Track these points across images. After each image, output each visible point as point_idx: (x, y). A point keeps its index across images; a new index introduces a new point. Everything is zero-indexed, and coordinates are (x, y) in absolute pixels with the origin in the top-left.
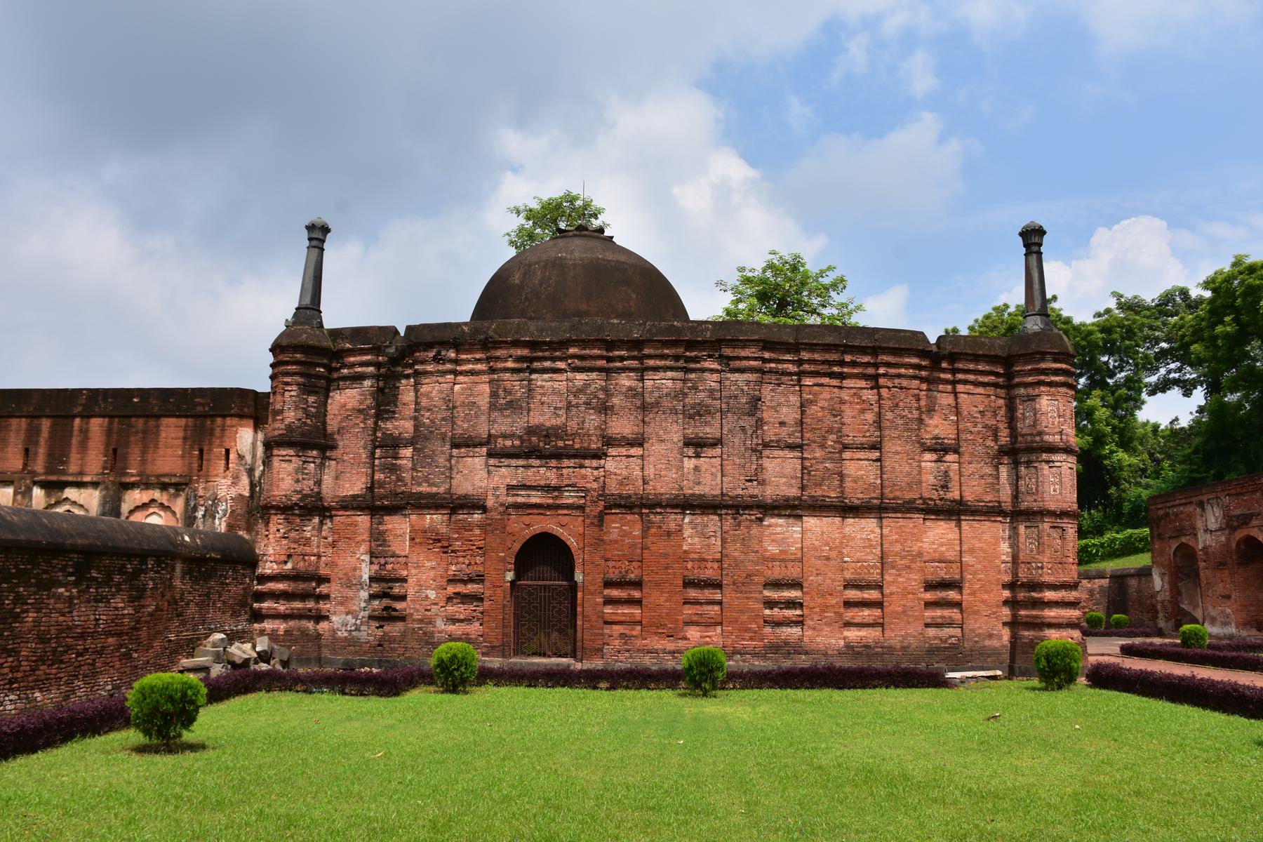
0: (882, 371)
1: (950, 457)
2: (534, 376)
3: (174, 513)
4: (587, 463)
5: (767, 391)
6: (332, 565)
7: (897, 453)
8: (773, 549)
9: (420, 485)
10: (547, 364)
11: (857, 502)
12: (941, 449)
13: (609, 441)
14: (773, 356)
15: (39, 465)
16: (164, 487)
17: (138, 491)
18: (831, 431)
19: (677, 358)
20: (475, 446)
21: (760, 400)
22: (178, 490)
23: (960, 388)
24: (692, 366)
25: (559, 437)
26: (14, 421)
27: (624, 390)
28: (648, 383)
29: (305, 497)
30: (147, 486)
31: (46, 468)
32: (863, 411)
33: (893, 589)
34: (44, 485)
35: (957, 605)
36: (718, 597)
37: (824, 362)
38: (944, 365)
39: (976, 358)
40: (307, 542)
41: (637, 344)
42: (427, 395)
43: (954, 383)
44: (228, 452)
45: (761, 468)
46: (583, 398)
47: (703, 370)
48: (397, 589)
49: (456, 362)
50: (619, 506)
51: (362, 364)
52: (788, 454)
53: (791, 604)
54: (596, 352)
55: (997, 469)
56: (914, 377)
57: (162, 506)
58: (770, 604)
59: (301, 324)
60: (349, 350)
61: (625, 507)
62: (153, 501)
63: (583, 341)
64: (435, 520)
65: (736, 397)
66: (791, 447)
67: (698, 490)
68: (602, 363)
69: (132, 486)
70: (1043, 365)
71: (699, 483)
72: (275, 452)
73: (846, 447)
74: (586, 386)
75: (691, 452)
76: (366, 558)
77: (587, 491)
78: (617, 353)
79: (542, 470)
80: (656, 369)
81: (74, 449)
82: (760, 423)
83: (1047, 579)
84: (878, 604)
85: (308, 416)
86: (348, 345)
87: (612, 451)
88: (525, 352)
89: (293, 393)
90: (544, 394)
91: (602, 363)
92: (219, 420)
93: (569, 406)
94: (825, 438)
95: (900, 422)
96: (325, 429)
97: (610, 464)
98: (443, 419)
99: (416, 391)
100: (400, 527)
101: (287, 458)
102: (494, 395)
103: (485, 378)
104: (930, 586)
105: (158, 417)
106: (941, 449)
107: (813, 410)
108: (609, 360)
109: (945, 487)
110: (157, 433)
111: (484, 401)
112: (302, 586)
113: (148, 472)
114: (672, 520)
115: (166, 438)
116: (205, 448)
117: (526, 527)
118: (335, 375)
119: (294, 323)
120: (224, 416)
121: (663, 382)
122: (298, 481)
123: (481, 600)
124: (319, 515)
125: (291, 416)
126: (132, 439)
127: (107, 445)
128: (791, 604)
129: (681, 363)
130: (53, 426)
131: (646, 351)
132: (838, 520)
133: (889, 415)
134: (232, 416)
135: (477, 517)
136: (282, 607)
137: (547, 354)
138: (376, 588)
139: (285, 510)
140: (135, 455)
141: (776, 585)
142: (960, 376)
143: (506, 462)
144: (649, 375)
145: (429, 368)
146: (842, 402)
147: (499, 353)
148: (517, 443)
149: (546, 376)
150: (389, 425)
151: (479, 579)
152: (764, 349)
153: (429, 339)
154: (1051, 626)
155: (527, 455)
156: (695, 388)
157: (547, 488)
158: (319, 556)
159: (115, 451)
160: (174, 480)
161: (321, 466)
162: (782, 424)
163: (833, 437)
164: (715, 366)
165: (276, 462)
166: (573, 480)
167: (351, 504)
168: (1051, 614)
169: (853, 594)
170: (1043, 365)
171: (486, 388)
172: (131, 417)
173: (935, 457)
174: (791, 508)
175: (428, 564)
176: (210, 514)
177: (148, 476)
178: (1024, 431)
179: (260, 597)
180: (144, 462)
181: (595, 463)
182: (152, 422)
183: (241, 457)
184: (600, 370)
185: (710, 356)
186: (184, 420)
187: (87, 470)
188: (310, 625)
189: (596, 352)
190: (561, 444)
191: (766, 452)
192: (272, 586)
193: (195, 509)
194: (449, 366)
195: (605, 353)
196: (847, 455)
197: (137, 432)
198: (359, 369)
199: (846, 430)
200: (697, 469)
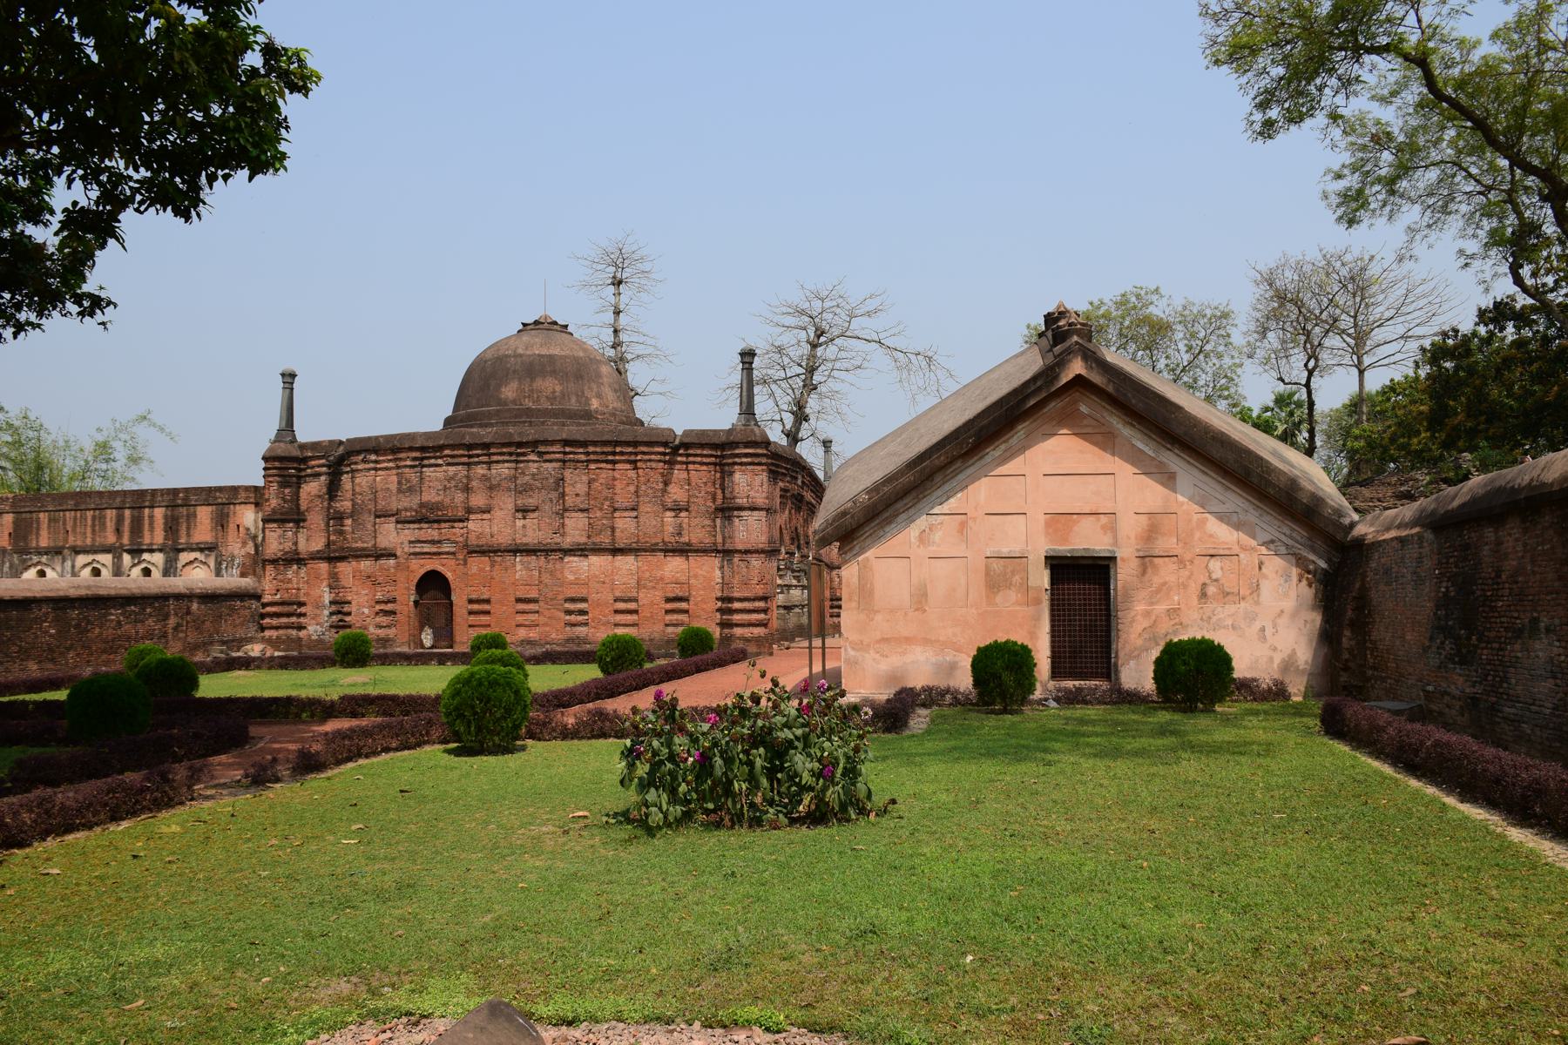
0: (639, 457)
1: (683, 514)
2: (424, 469)
4: (456, 525)
5: (567, 473)
6: (307, 594)
7: (647, 512)
8: (571, 577)
9: (356, 542)
10: (433, 461)
11: (622, 546)
12: (677, 509)
13: (469, 511)
14: (572, 450)
15: (126, 540)
16: (201, 550)
18: (606, 499)
19: (511, 454)
20: (390, 516)
21: (562, 479)
24: (522, 458)
25: (439, 509)
27: (479, 476)
28: (494, 471)
29: (287, 553)
30: (193, 550)
32: (628, 484)
33: (645, 602)
34: (129, 552)
35: (686, 612)
36: (537, 608)
37: (603, 453)
38: (681, 451)
39: (702, 446)
40: (290, 581)
41: (486, 446)
42: (359, 484)
44: (238, 526)
45: (563, 525)
46: (453, 483)
47: (528, 461)
48: (346, 608)
49: (376, 462)
50: (476, 552)
51: (319, 466)
52: (580, 515)
53: (582, 612)
54: (461, 452)
55: (714, 521)
56: (660, 461)
58: (569, 612)
59: (279, 441)
60: (310, 457)
61: (479, 552)
62: (196, 559)
63: (452, 445)
64: (366, 565)
65: (547, 478)
66: (582, 511)
67: (525, 540)
68: (465, 460)
69: (183, 550)
70: (737, 451)
71: (525, 536)
73: (615, 510)
74: (456, 475)
75: (519, 515)
76: (327, 589)
77: (457, 543)
78: (475, 452)
79: (429, 530)
80: (498, 462)
82: (563, 495)
83: (736, 595)
84: (635, 612)
85: (285, 501)
86: (310, 454)
87: (472, 517)
88: (417, 454)
91: (465, 460)
92: (232, 506)
93: (445, 488)
94: (603, 504)
95: (650, 491)
96: (298, 508)
97: (471, 525)
98: (370, 500)
99: (353, 482)
100: (345, 569)
102: (399, 483)
103: (394, 472)
104: (668, 600)
106: (677, 509)
108: (470, 456)
109: (680, 534)
110: (195, 516)
111: (394, 487)
112: (286, 609)
114: (509, 558)
117: (421, 567)
118: (303, 474)
119: (275, 441)
120: (235, 504)
121: (503, 470)
122: (281, 543)
123: (395, 613)
124: (297, 564)
125: (274, 503)
128: (582, 612)
129: (513, 458)
131: (492, 451)
132: (610, 557)
133: (643, 487)
134: (242, 503)
135: (392, 562)
136: (275, 622)
137: (432, 454)
138: (334, 608)
139: (274, 562)
141: (573, 600)
142: (691, 459)
143: (407, 526)
144: (494, 466)
145: (359, 467)
146: (614, 479)
147: (402, 455)
148: (414, 513)
149: (432, 469)
150: (338, 505)
151: (393, 601)
152: (564, 446)
153: (358, 448)
154: (737, 625)
155: (419, 521)
156: (523, 473)
157: (433, 542)
158: (298, 589)
161: (296, 534)
162: (577, 495)
163: (608, 503)
164: (536, 458)
165: (267, 531)
166: (448, 537)
167: (316, 557)
168: (737, 617)
169: (621, 606)
170: (737, 451)
171: (395, 478)
173: (673, 514)
174: (581, 551)
175: (364, 592)
179: (263, 616)
180: (188, 535)
181: (461, 525)
183: (248, 529)
184: (463, 464)
185: (533, 452)
188: (294, 632)
189: (461, 452)
190: (440, 513)
191: (567, 514)
192: (269, 609)
193: (220, 564)
194: (372, 465)
195: (466, 453)
196: (617, 514)
199: (617, 498)
200: (524, 526)
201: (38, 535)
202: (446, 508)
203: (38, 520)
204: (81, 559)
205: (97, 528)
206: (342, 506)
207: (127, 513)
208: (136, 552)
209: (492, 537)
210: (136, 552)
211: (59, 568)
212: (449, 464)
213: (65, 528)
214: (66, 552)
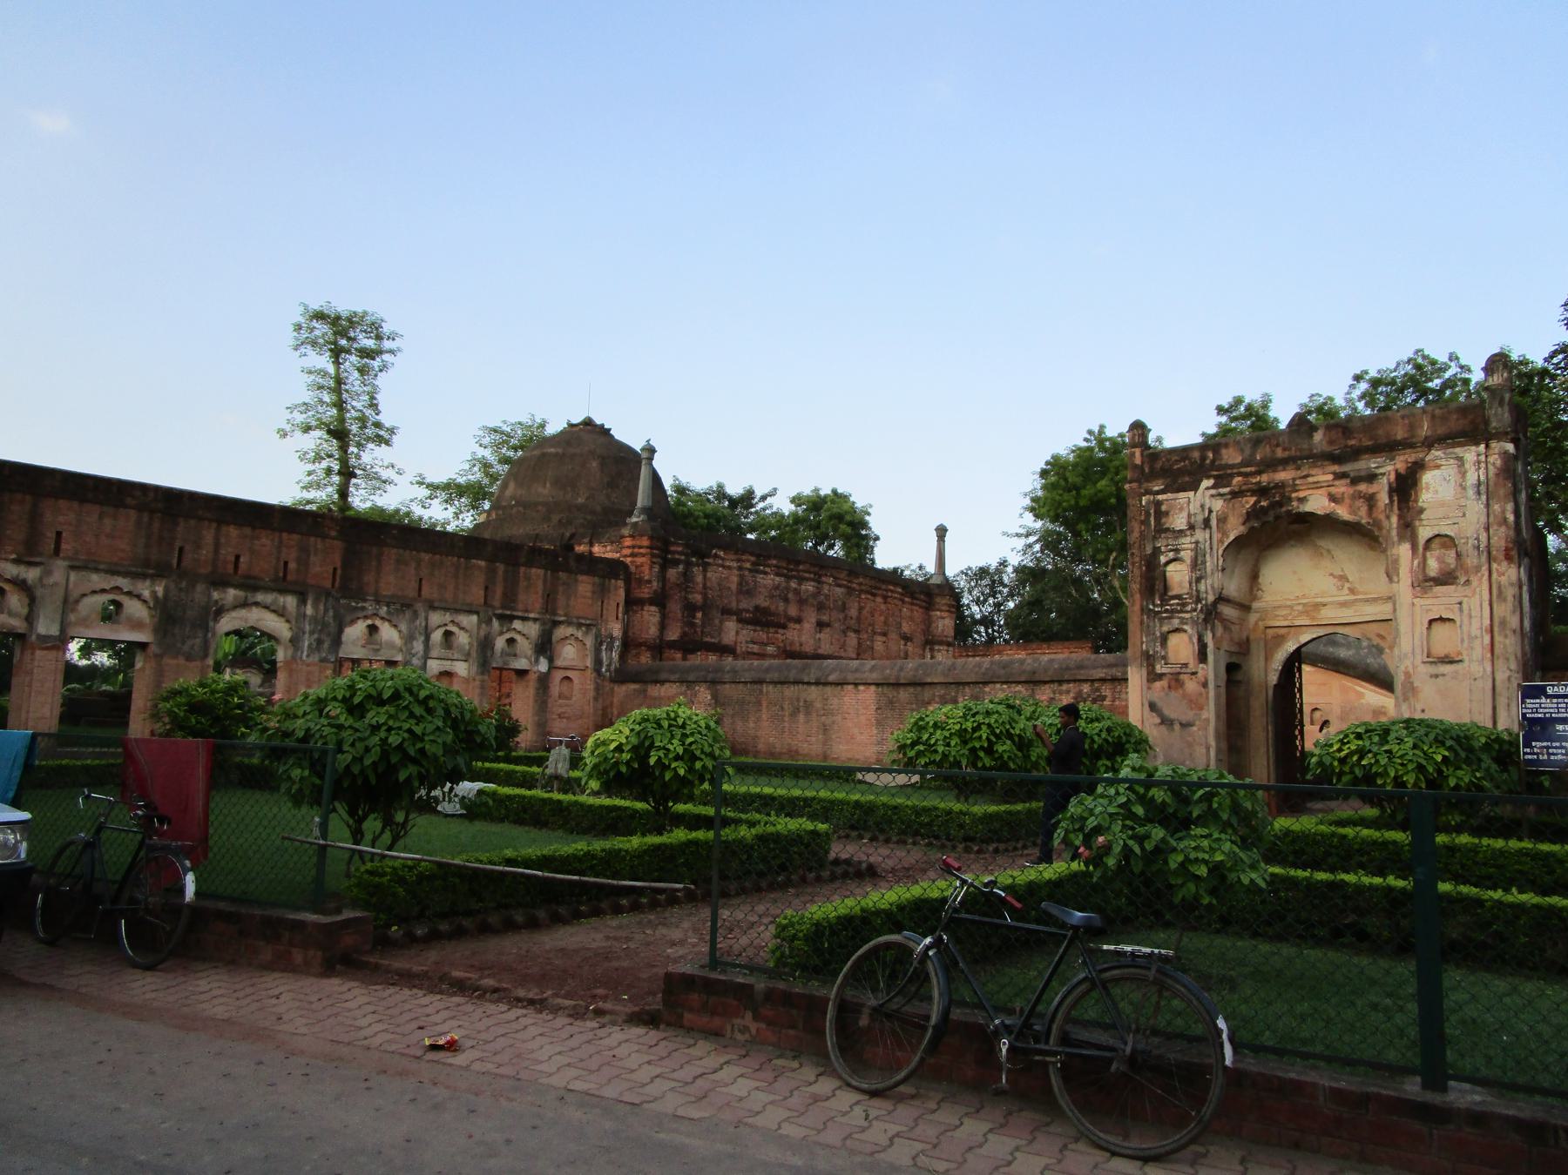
0: (890, 594)
16: (579, 625)
18: (870, 625)
23: (915, 608)
28: (803, 587)
30: (569, 623)
34: (501, 617)
42: (710, 579)
51: (678, 553)
73: (875, 633)
91: (785, 571)
92: (613, 581)
102: (740, 584)
105: (576, 574)
107: (865, 612)
111: (734, 587)
116: (606, 601)
140: (561, 600)
145: (711, 560)
147: (744, 557)
159: (548, 595)
160: (588, 622)
163: (870, 628)
171: (735, 579)
193: (601, 644)
194: (720, 562)
202: (773, 614)
204: (436, 618)
207: (501, 567)
208: (507, 619)
209: (801, 645)
211: (403, 627)
212: (777, 575)
214: (419, 606)
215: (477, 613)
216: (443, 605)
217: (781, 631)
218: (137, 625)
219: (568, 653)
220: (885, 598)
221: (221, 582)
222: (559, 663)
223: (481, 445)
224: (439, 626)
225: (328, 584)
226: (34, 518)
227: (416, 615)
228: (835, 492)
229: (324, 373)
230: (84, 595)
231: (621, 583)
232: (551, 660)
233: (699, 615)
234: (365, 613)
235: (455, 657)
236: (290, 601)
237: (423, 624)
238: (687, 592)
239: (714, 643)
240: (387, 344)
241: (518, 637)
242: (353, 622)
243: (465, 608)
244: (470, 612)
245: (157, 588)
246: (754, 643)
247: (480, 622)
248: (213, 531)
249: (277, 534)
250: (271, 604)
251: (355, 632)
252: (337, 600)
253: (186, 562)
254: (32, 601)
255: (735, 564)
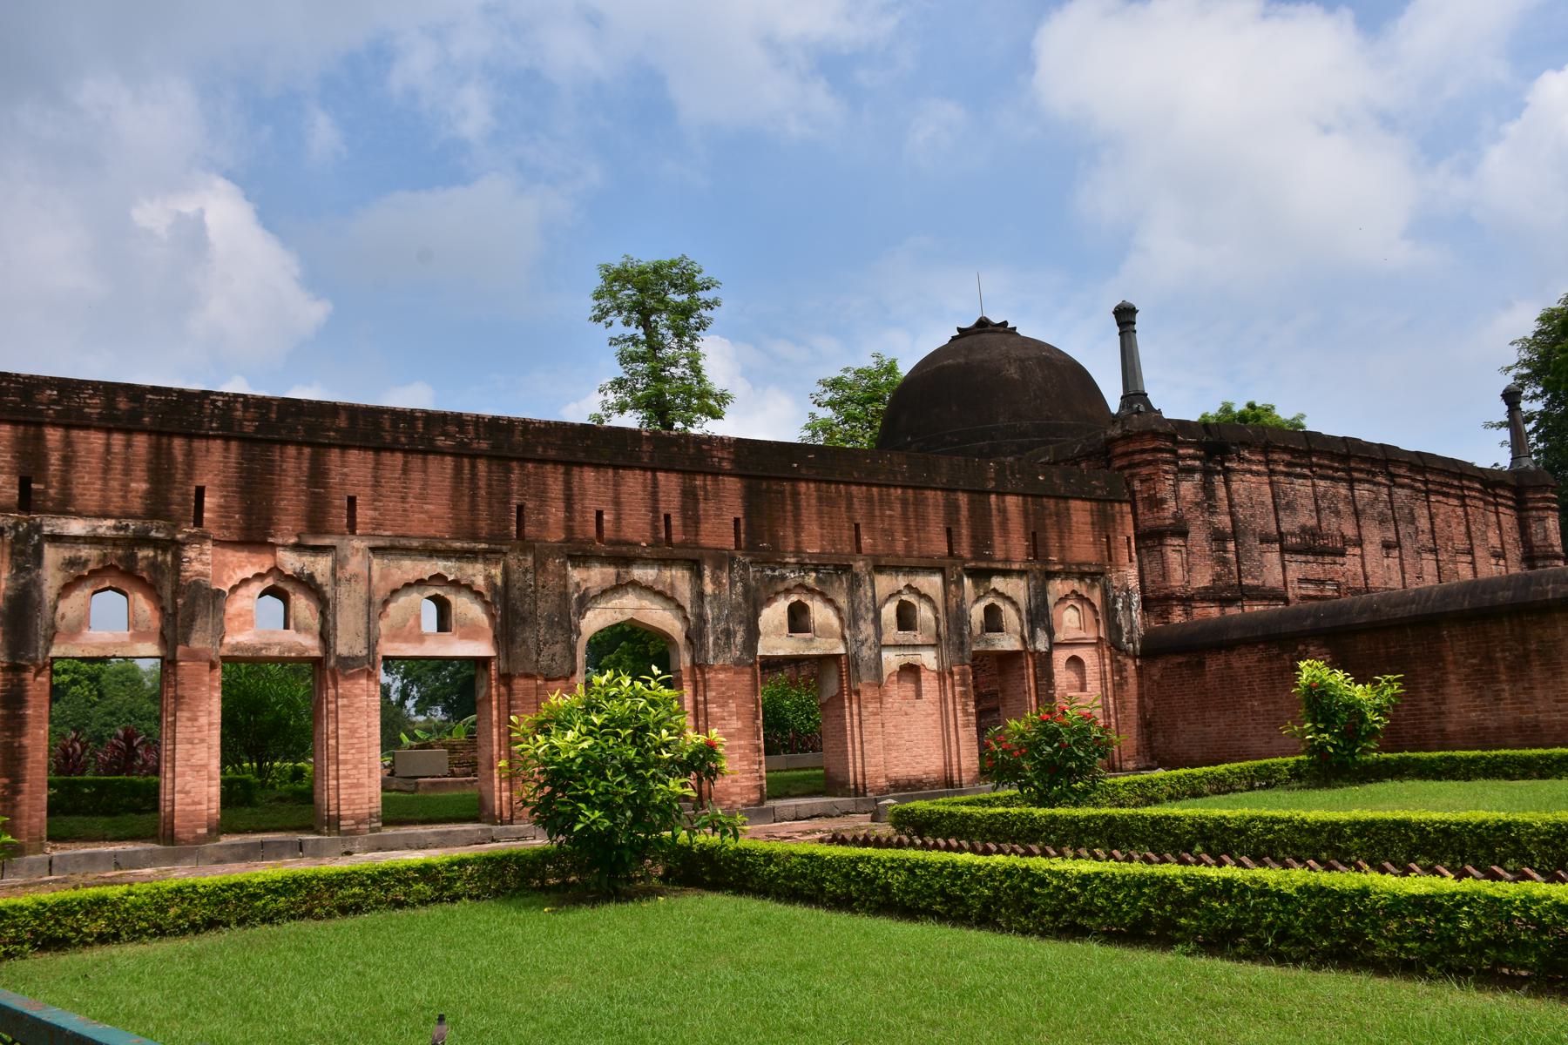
3: (1092, 605)
10: (1299, 470)
15: (965, 550)
16: (1081, 577)
17: (1059, 581)
19: (1368, 472)
22: (1093, 580)
26: (930, 494)
30: (1067, 574)
31: (972, 552)
32: (1459, 524)
37: (1440, 484)
43: (1497, 505)
57: (1080, 598)
72: (1169, 541)
81: (996, 532)
89: (1171, 482)
90: (1301, 497)
98: (1251, 516)
101: (1178, 548)
105: (1066, 498)
110: (1069, 516)
113: (1068, 560)
115: (1077, 522)
126: (1048, 522)
127: (1026, 527)
130: (971, 502)
137: (1298, 461)
147: (1276, 457)
148: (1299, 540)
149: (1300, 481)
160: (1093, 569)
163: (1450, 543)
171: (1267, 488)
172: (1041, 496)
176: (1128, 607)
177: (1070, 564)
178: (1539, 543)
180: (1062, 548)
182: (1062, 505)
186: (1089, 503)
187: (1012, 556)
190: (1322, 542)
193: (1115, 601)
197: (1051, 515)
198: (1189, 462)
201: (798, 530)
203: (795, 494)
204: (885, 583)
205: (912, 522)
206: (1220, 522)
208: (981, 576)
210: (981, 576)
211: (843, 601)
213: (851, 519)
215: (941, 570)
216: (893, 561)
217: (1339, 560)
218: (471, 633)
219: (1070, 621)
220: (1462, 498)
221: (582, 558)
222: (1060, 636)
223: (819, 405)
224: (891, 596)
225: (730, 543)
226: (317, 476)
227: (855, 584)
228: (1251, 406)
229: (634, 340)
230: (395, 592)
231: (1127, 508)
232: (1050, 632)
233: (1231, 546)
234: (786, 585)
235: (919, 640)
236: (679, 578)
237: (870, 594)
238: (1212, 514)
239: (1258, 586)
240: (703, 295)
241: (999, 603)
242: (769, 601)
243: (924, 563)
244: (931, 569)
245: (493, 571)
246: (1307, 581)
247: (945, 583)
248: (561, 477)
249: (649, 474)
250: (655, 581)
251: (774, 614)
252: (745, 568)
253: (530, 530)
254: (324, 604)
255: (1262, 468)
